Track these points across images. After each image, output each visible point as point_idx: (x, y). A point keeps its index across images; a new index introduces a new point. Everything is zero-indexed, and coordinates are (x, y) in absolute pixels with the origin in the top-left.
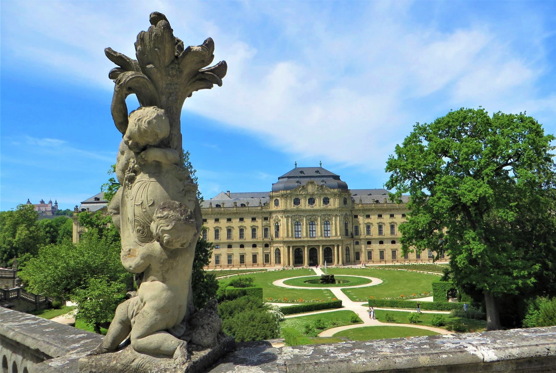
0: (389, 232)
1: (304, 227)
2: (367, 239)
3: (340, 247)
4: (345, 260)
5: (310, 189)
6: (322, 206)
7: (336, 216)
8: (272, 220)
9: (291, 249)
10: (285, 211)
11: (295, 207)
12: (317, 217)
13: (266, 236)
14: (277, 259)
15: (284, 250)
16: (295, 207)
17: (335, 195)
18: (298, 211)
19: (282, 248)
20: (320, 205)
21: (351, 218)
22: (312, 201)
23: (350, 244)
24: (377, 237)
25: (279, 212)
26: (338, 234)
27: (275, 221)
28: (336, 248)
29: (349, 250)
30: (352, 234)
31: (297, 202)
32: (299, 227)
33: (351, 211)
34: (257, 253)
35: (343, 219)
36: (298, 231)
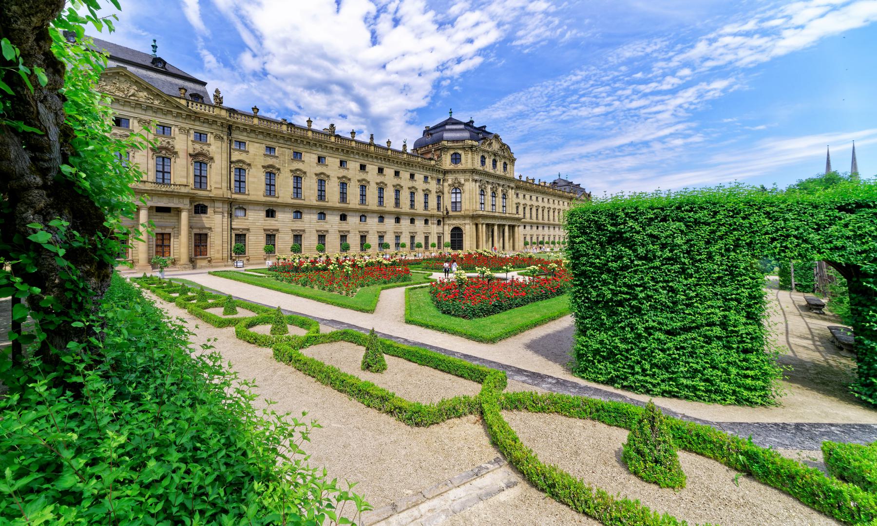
8: (446, 184)
10: (474, 171)
16: (481, 168)
25: (464, 171)
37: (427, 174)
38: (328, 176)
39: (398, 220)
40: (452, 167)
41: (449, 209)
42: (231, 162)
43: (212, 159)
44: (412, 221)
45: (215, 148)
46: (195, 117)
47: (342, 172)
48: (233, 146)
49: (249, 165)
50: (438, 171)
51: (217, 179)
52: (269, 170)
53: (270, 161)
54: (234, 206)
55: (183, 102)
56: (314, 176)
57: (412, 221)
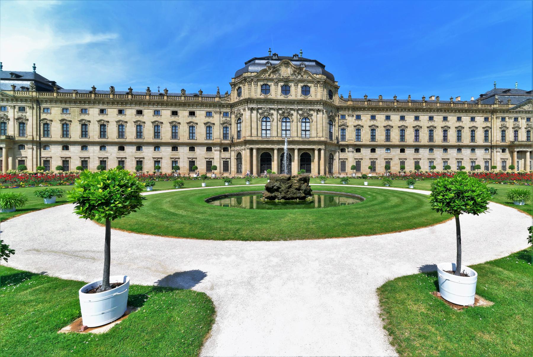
1: (275, 123)
3: (322, 152)
4: (327, 170)
5: (286, 72)
7: (318, 111)
15: (246, 154)
16: (262, 97)
17: (319, 82)
18: (267, 101)
22: (286, 90)
26: (320, 134)
27: (236, 116)
28: (316, 152)
31: (265, 89)
32: (268, 124)
36: (266, 130)
38: (108, 122)
39: (175, 148)
40: (237, 100)
42: (40, 121)
43: (28, 120)
44: (192, 149)
45: (30, 114)
46: (15, 99)
47: (121, 117)
48: (42, 111)
49: (51, 121)
50: (221, 106)
51: (31, 131)
52: (64, 122)
53: (65, 117)
54: (42, 145)
55: (12, 93)
56: (97, 123)
57: (192, 149)
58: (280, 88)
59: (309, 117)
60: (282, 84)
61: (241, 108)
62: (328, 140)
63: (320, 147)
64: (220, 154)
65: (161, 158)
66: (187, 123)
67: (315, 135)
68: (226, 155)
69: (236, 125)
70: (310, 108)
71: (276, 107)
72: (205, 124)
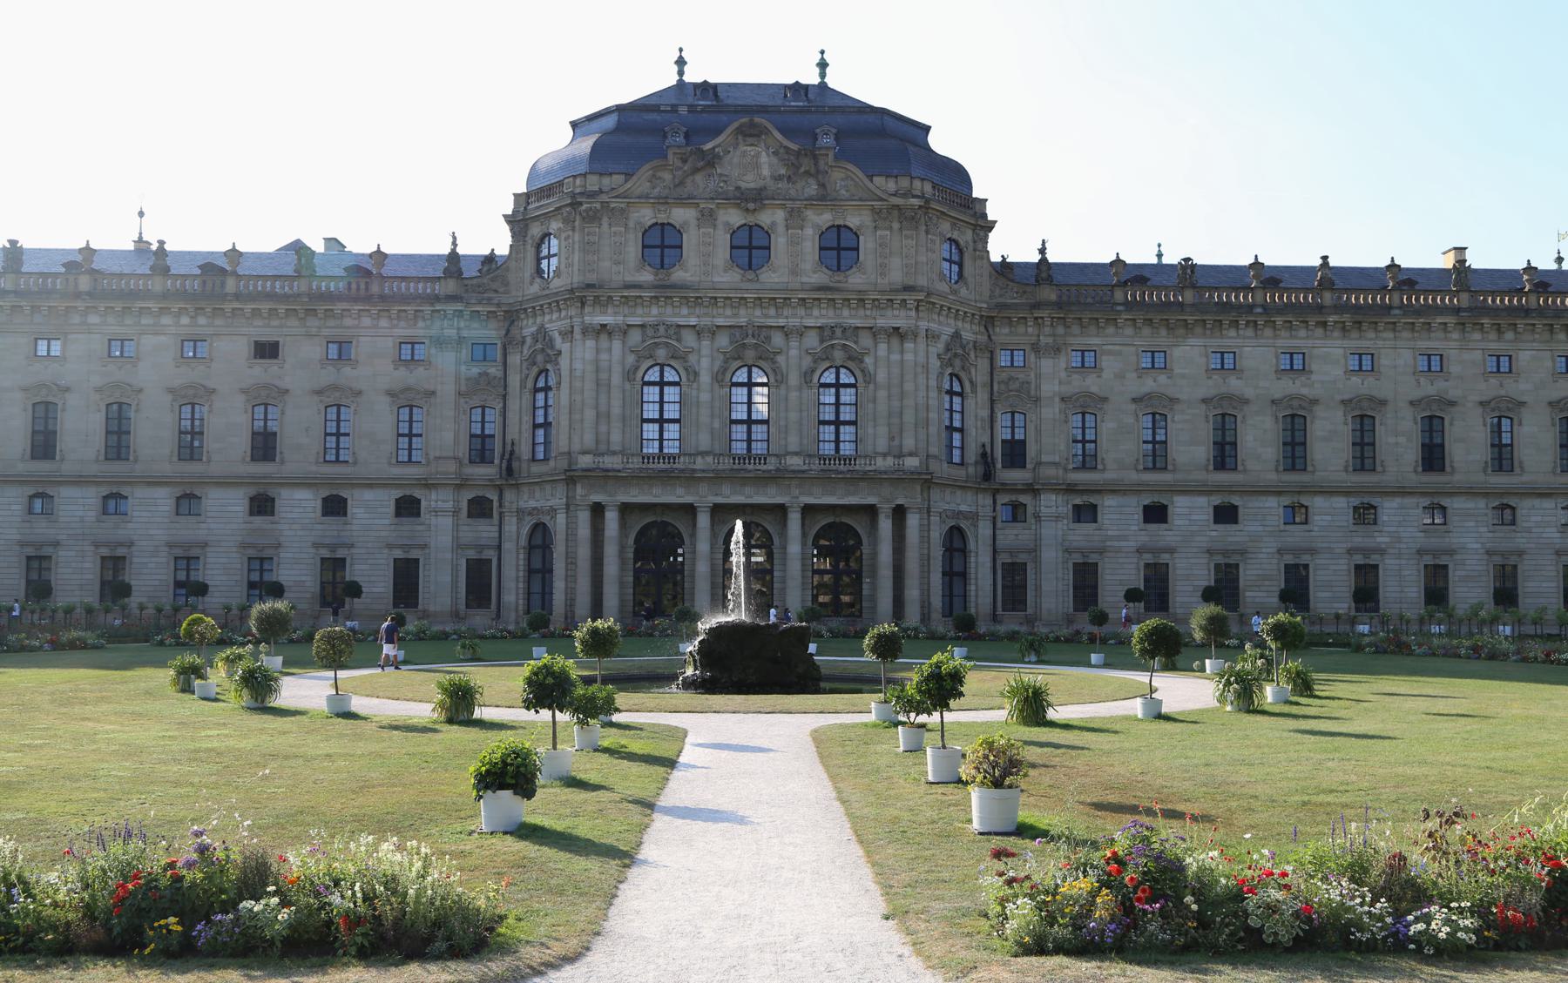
0: (1202, 452)
2: (1071, 489)
3: (913, 521)
6: (813, 275)
8: (515, 359)
9: (611, 518)
10: (586, 294)
11: (647, 276)
12: (778, 340)
13: (481, 449)
14: (537, 588)
16: (647, 276)
19: (561, 518)
20: (794, 272)
21: (983, 364)
22: (751, 248)
23: (974, 517)
24: (1133, 476)
25: (556, 302)
28: (885, 525)
29: (964, 551)
30: (985, 458)
31: (662, 245)
33: (988, 322)
34: (424, 547)
35: (935, 363)
37: (403, 331)
41: (524, 451)
58: (723, 239)
59: (850, 364)
60: (735, 218)
61: (554, 323)
62: (940, 469)
63: (900, 502)
64: (456, 527)
65: (205, 545)
66: (319, 392)
67: (882, 445)
68: (485, 530)
69: (527, 396)
70: (858, 322)
71: (706, 321)
72: (391, 394)
